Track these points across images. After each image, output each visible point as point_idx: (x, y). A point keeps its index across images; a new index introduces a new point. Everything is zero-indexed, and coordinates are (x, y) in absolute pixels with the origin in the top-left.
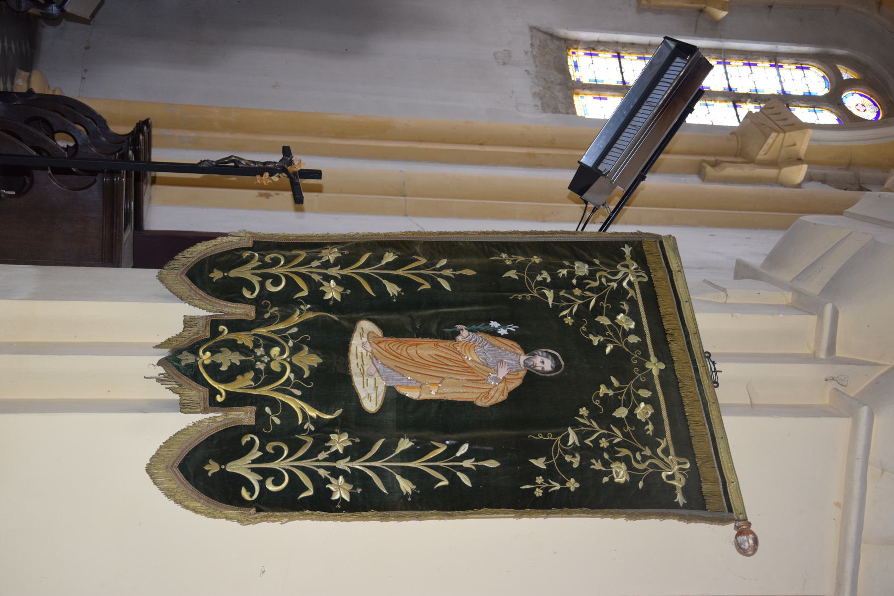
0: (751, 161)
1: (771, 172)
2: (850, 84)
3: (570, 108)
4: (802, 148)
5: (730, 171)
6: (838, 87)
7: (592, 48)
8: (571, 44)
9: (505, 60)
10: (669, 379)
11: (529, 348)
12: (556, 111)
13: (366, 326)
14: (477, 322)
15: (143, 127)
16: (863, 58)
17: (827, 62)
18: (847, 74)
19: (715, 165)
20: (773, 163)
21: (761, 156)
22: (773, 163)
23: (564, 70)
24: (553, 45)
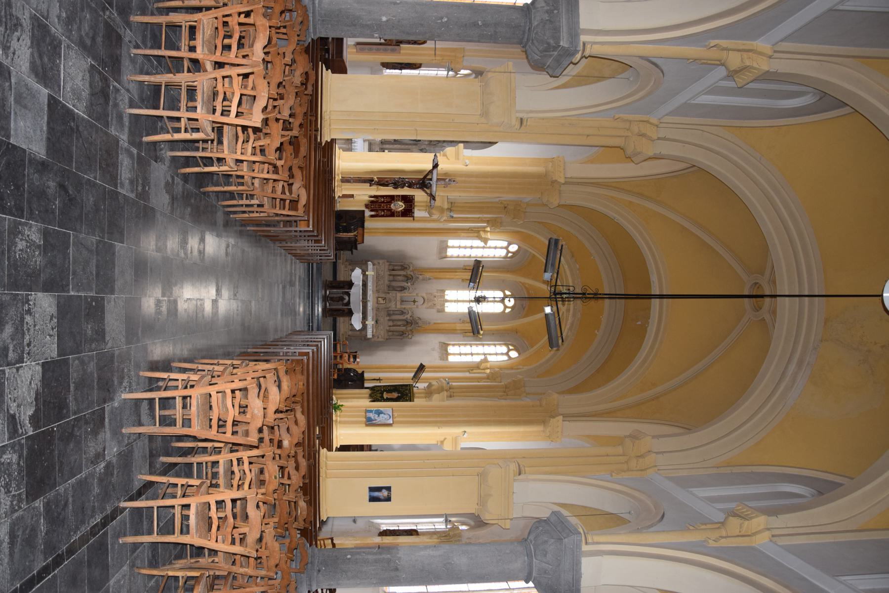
0: (479, 369)
1: (483, 371)
2: (512, 350)
3: (447, 359)
4: (489, 367)
5: (475, 371)
6: (509, 350)
7: (454, 345)
8: (448, 345)
9: (433, 350)
10: (410, 396)
11: (398, 393)
12: (444, 360)
13: (385, 393)
14: (394, 392)
15: (363, 372)
16: (515, 344)
17: (507, 345)
18: (511, 347)
19: (472, 370)
20: (484, 369)
21: (481, 368)
22: (484, 369)
23: (447, 351)
24: (444, 345)
